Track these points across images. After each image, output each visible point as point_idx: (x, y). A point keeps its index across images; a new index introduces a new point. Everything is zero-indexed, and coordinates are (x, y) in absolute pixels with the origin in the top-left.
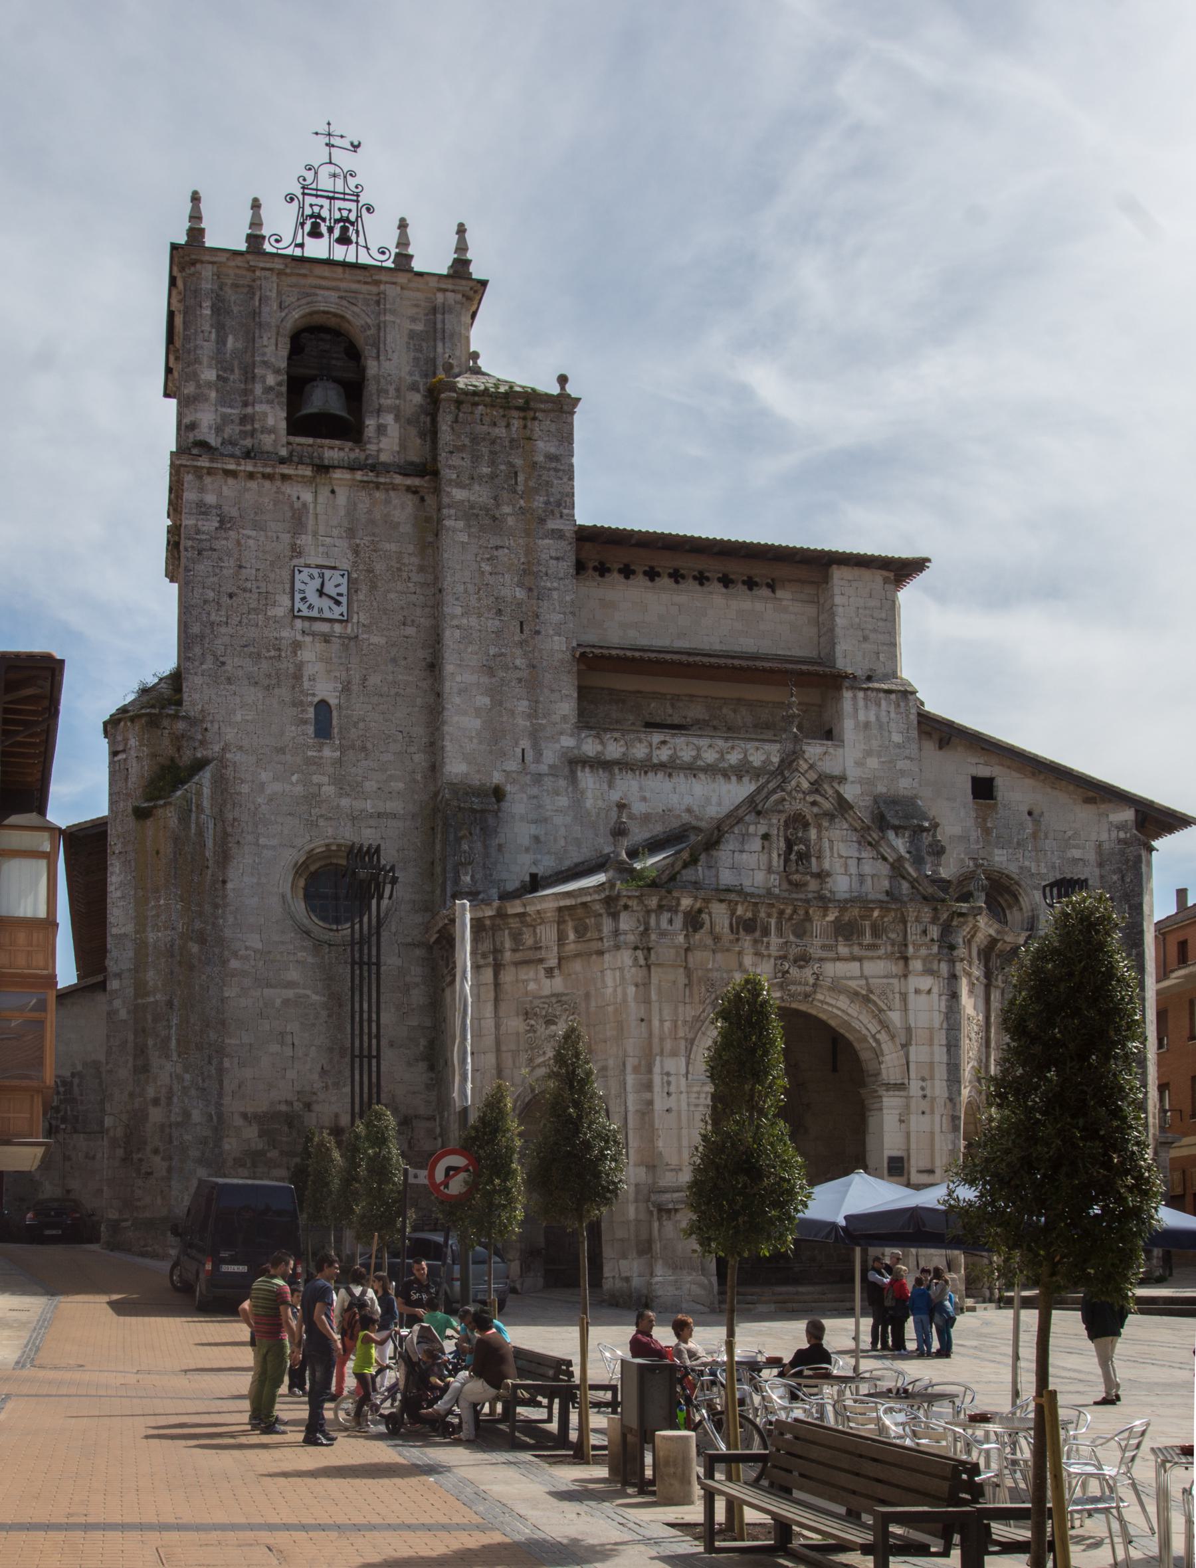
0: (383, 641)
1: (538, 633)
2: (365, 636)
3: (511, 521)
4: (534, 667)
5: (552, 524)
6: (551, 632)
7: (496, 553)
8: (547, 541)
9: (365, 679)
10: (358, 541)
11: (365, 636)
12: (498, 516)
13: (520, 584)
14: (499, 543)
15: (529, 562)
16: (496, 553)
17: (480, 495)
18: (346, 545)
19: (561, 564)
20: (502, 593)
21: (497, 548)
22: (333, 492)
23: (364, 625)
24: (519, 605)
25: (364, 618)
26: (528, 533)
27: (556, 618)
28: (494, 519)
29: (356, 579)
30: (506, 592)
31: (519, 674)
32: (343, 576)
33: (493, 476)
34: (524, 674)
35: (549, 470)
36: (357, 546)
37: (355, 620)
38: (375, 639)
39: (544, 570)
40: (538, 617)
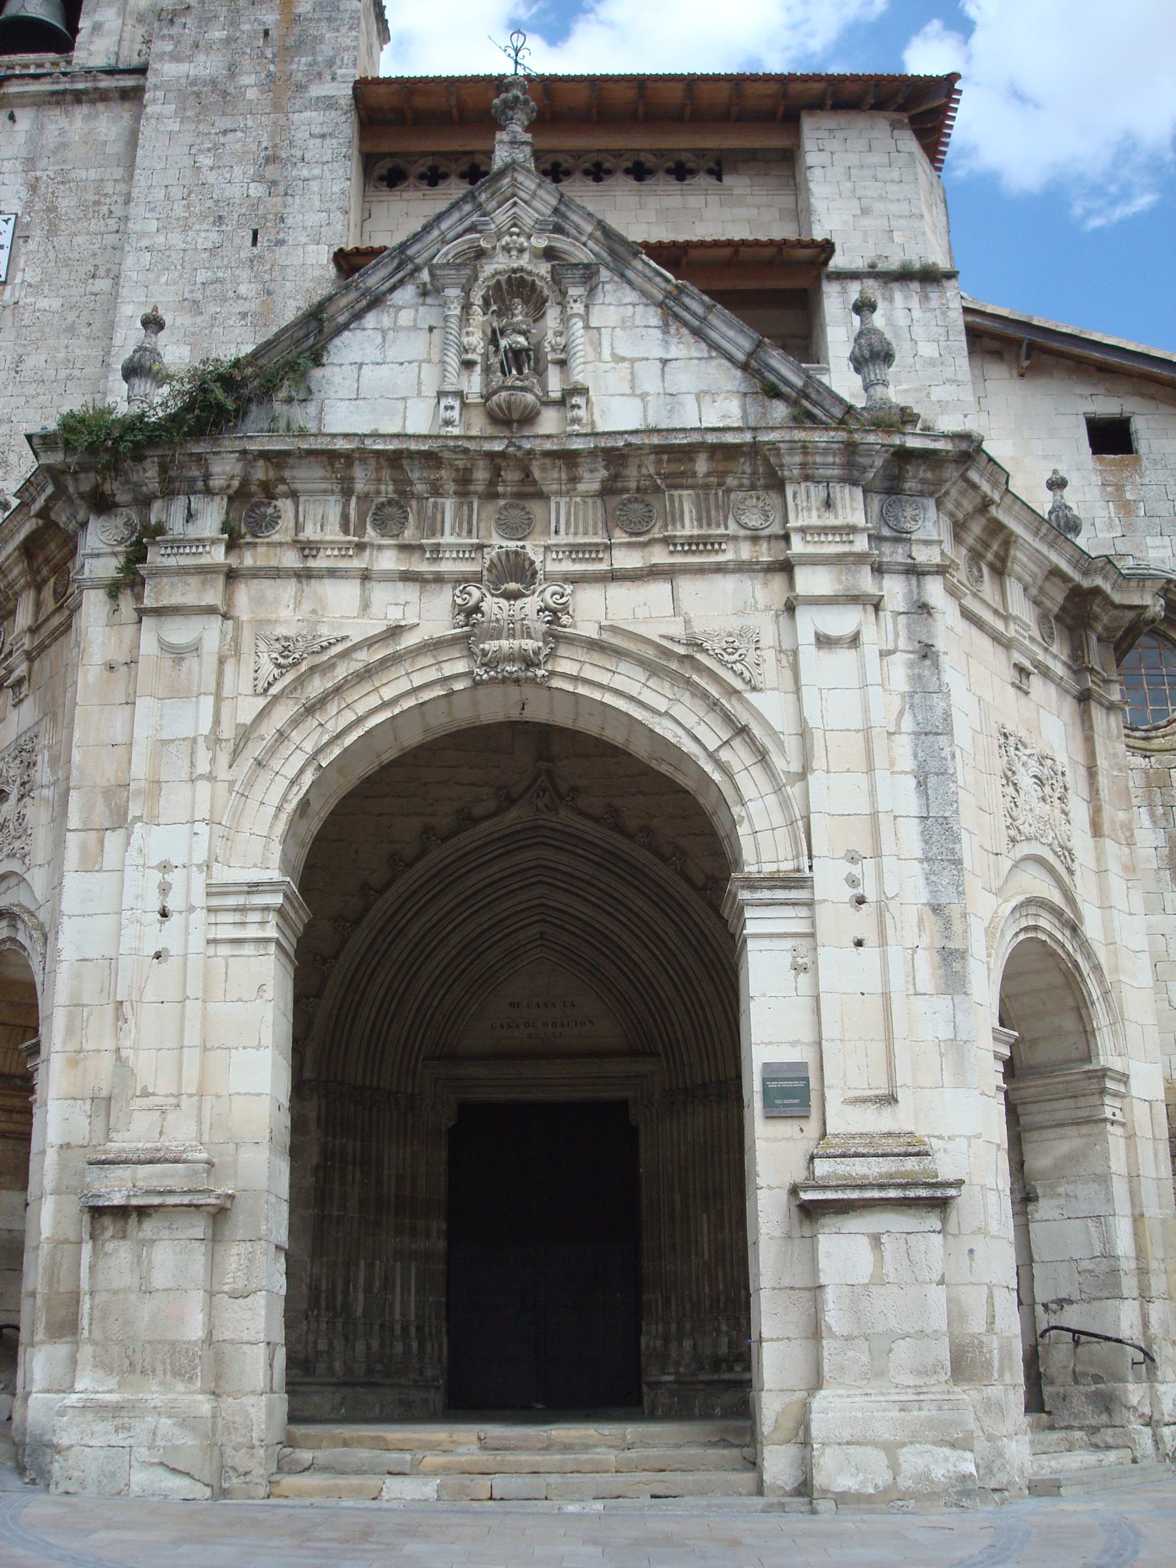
0: (56, 304)
1: (281, 243)
2: (30, 300)
3: (252, 94)
4: (269, 293)
5: (316, 91)
6: (304, 240)
7: (222, 140)
8: (307, 114)
9: (21, 360)
10: (39, 174)
11: (30, 300)
12: (231, 90)
13: (259, 178)
14: (230, 126)
15: (275, 146)
16: (222, 140)
17: (207, 66)
18: (20, 181)
19: (328, 142)
20: (227, 194)
21: (225, 133)
22: (12, 117)
23: (30, 285)
24: (254, 207)
25: (31, 275)
26: (277, 107)
27: (314, 219)
28: (225, 94)
29: (28, 224)
30: (235, 192)
31: (242, 307)
32: (6, 221)
33: (228, 41)
34: (254, 306)
35: (319, 20)
36: (37, 179)
37: (18, 280)
38: (43, 303)
39: (299, 154)
40: (282, 220)
